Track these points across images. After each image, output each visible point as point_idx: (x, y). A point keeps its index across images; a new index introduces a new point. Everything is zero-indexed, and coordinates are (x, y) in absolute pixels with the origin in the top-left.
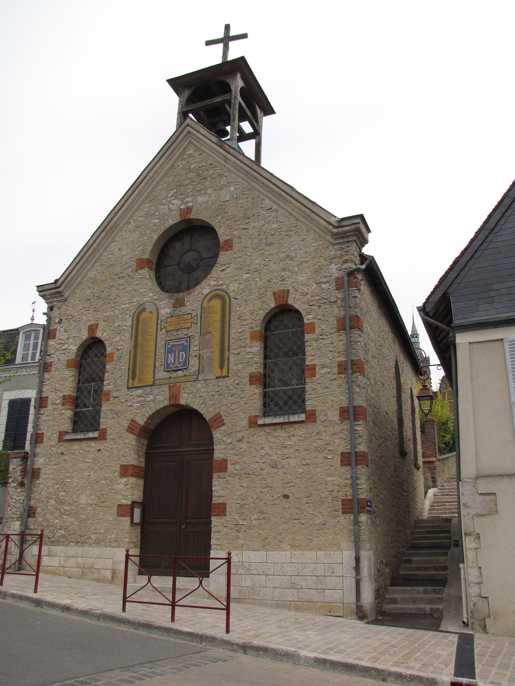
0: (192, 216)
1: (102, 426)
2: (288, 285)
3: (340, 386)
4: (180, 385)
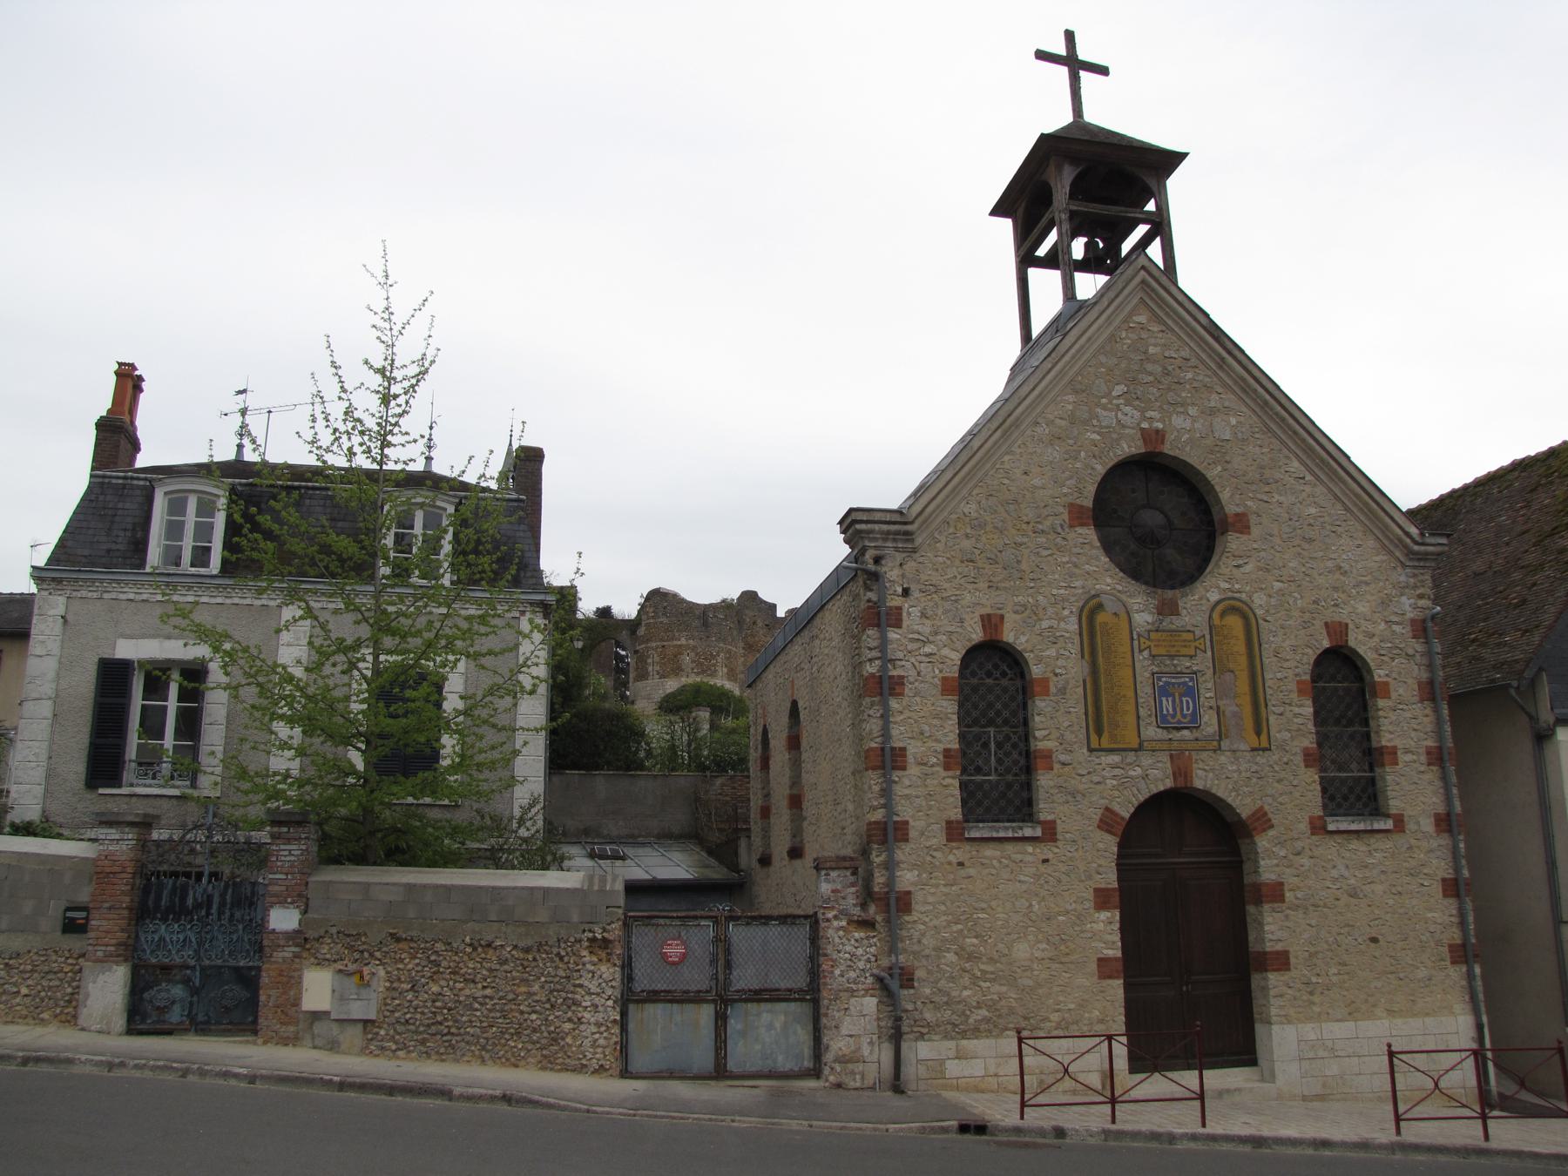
0: (1167, 449)
1: (1043, 817)
2: (1343, 615)
3: (1430, 783)
4: (1190, 757)
